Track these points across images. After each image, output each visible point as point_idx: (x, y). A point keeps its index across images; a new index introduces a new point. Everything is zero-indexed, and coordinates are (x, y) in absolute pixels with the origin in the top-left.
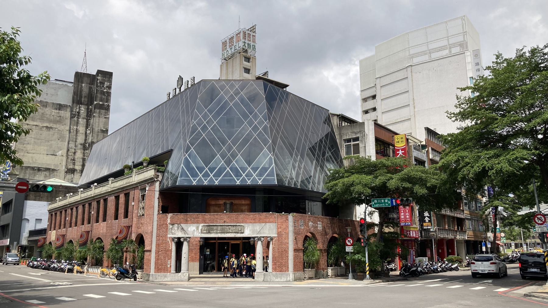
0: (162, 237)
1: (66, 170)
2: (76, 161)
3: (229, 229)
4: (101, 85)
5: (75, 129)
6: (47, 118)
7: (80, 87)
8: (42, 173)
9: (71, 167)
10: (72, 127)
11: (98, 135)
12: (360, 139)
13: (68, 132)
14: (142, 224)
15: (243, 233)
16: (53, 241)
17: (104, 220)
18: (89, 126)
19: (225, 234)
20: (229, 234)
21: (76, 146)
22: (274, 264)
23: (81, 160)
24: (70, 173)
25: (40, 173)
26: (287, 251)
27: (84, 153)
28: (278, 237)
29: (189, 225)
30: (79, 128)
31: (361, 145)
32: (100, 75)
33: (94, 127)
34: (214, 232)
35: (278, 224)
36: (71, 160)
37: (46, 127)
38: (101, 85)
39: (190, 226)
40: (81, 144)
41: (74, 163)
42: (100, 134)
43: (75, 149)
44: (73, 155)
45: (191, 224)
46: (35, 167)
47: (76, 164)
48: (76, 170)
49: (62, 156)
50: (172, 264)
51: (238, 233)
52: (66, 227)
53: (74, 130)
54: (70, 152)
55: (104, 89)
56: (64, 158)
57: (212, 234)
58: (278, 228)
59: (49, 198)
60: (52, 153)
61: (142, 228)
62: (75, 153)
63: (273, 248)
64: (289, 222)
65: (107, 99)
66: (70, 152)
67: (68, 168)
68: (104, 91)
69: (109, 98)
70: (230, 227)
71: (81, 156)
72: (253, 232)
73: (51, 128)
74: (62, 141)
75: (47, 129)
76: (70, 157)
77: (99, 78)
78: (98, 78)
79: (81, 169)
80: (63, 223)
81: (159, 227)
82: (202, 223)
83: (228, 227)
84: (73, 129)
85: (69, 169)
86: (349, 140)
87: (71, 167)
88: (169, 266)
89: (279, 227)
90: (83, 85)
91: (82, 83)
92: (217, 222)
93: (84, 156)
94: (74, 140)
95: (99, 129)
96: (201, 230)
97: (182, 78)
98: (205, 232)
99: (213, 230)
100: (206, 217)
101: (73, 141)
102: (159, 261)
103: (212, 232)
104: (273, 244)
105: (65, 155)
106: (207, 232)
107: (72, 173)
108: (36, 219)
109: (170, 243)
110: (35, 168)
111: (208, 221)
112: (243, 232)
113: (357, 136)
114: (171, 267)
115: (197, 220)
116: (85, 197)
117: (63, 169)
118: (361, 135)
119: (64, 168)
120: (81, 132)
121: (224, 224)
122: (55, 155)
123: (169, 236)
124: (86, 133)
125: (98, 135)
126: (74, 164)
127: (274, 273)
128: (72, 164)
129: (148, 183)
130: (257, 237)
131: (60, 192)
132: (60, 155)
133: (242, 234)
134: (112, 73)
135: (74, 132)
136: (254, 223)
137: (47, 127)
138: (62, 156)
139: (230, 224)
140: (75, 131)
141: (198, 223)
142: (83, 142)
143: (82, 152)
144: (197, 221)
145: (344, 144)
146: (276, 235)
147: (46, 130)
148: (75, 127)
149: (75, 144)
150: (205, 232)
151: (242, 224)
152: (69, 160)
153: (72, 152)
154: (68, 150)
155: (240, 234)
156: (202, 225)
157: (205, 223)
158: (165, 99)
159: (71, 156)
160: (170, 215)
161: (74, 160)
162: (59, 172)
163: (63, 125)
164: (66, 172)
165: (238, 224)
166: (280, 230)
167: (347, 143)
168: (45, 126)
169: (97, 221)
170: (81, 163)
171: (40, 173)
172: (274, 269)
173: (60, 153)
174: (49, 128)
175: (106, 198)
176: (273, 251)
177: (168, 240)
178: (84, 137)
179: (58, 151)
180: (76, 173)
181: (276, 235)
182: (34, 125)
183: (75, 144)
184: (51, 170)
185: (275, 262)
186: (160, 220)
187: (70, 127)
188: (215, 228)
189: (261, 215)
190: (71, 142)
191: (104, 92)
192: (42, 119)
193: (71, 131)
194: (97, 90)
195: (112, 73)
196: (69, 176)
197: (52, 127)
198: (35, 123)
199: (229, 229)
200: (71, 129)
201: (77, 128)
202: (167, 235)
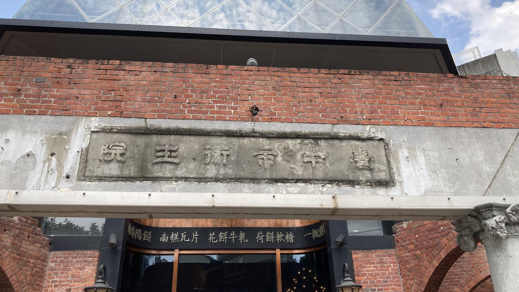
3: (289, 155)
19: (264, 186)
20: (293, 188)
34: (179, 173)
45: (15, 119)
51: (352, 183)
57: (166, 185)
70: (290, 143)
82: (98, 112)
83: (277, 145)
98: (114, 169)
103: (167, 171)
106: (131, 170)
112: (383, 176)
115: (64, 92)
121: (247, 126)
130: (502, 208)
133: (381, 191)
136: (447, 124)
139: (288, 128)
141: (66, 112)
150: (114, 169)
155: (367, 190)
156: (95, 123)
157: (121, 115)
165: (343, 130)
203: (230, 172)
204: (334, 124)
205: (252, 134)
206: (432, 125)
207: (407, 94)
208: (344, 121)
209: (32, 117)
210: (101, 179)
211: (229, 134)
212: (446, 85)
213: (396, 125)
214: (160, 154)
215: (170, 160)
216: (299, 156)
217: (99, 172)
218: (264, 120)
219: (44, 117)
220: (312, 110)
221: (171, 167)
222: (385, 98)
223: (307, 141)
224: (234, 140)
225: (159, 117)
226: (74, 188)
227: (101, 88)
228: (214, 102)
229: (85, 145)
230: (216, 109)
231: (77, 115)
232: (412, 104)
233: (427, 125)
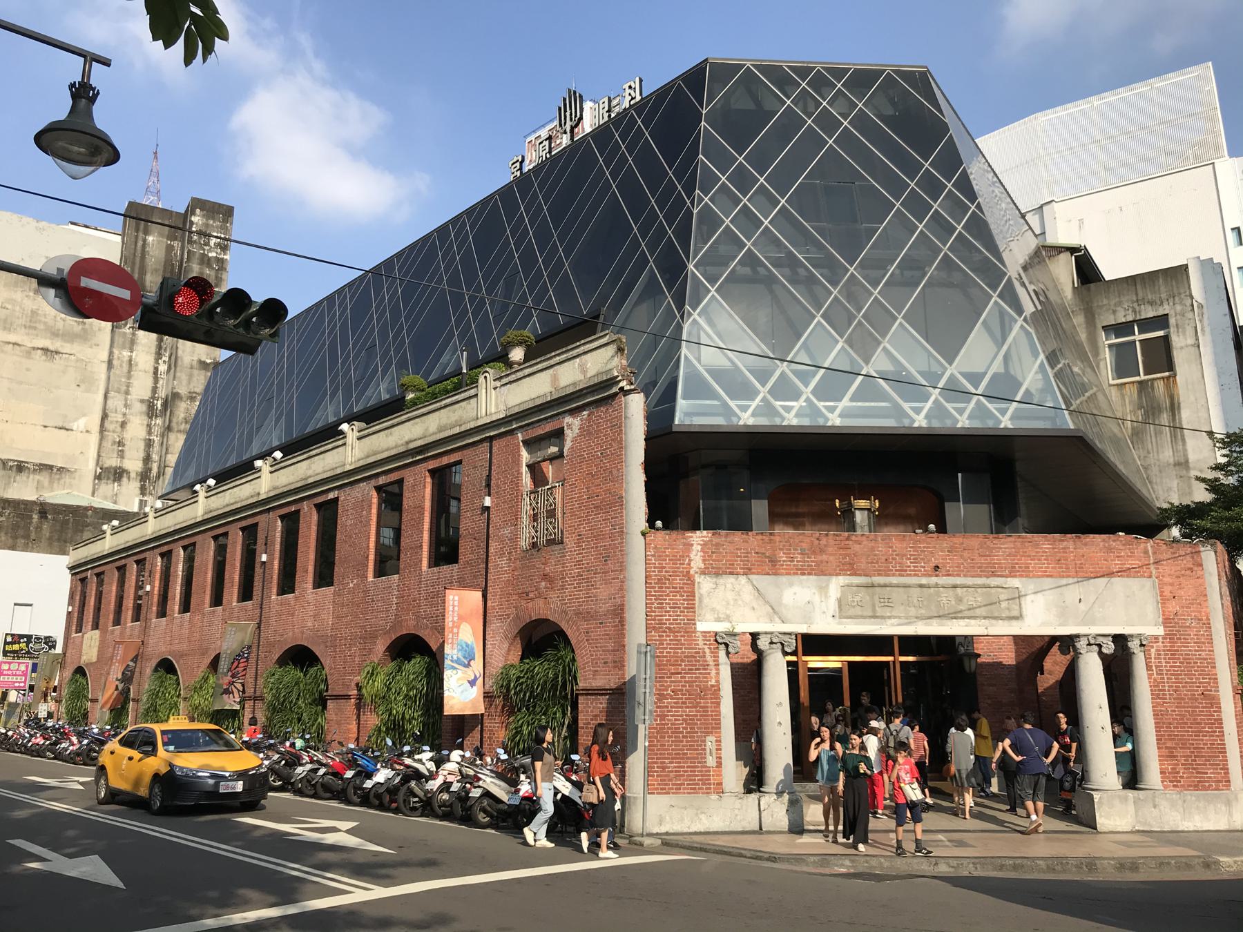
0: (669, 628)
1: (99, 470)
2: (126, 448)
4: (200, 238)
5: (126, 359)
6: (45, 323)
7: (140, 243)
8: (28, 477)
9: (112, 461)
10: (116, 351)
11: (190, 376)
12: (1172, 321)
13: (105, 366)
14: (545, 577)
15: (1019, 617)
16: (89, 664)
17: (324, 577)
18: (165, 350)
20: (962, 622)
21: (126, 406)
22: (1167, 755)
23: (142, 445)
24: (108, 479)
25: (25, 478)
26: (1213, 702)
27: (149, 426)
28: (1170, 636)
29: (784, 579)
30: (136, 356)
31: (1177, 341)
32: (198, 211)
33: (180, 352)
35: (1162, 584)
36: (114, 443)
37: (42, 349)
38: (200, 238)
39: (791, 585)
40: (142, 401)
41: (122, 451)
42: (196, 372)
43: (124, 415)
44: (119, 429)
46: (11, 460)
47: (127, 454)
48: (128, 472)
49: (87, 431)
50: (724, 754)
52: (142, 617)
53: (122, 362)
54: (111, 422)
55: (210, 251)
56: (94, 438)
57: (889, 622)
58: (1164, 600)
59: (56, 544)
60: (60, 425)
61: (551, 594)
62: (123, 425)
63: (1156, 686)
64: (1207, 575)
65: (217, 277)
66: (111, 422)
67: (106, 466)
68: (210, 255)
69: (223, 277)
70: (959, 590)
71: (142, 433)
72: (1063, 614)
73: (57, 353)
74: (88, 390)
75: (46, 355)
76: (112, 436)
77: (194, 219)
78: (193, 219)
79: (140, 470)
80: (129, 603)
81: (656, 583)
84: (119, 358)
85: (107, 468)
86: (1121, 329)
87: (114, 465)
88: (711, 761)
89: (1167, 593)
90: (150, 239)
91: (146, 233)
92: (902, 572)
93: (150, 433)
94: (124, 388)
95: (196, 358)
96: (840, 601)
97: (581, 96)
98: (858, 611)
99: (887, 602)
100: (857, 547)
101: (119, 393)
102: (667, 741)
104: (1149, 668)
105: (96, 428)
107: (114, 481)
108: (15, 604)
109: (708, 657)
110: (11, 464)
111: (863, 566)
112: (1016, 613)
113: (1161, 312)
114: (719, 764)
115: (820, 558)
116: (227, 505)
117: (89, 467)
118: (1178, 308)
119: (91, 464)
120: (141, 366)
122: (67, 430)
123: (701, 627)
124: (156, 369)
125: (190, 376)
126: (121, 455)
127: (1173, 794)
128: (115, 455)
129: (572, 412)
131: (87, 526)
132: (82, 427)
133: (1014, 623)
134: (233, 208)
135: (121, 366)
137: (45, 350)
138: (87, 431)
140: (124, 365)
141: (823, 573)
142: (147, 395)
143: (145, 423)
144: (818, 564)
145: (1106, 341)
146: (1160, 631)
147: (44, 357)
148: (126, 353)
149: (126, 400)
150: (858, 611)
151: (1015, 582)
152: (107, 444)
153: (117, 422)
154: (104, 417)
156: (842, 580)
157: (855, 574)
158: (505, 177)
159: (114, 432)
160: (698, 538)
161: (120, 443)
162: (77, 475)
163: (91, 347)
164: (98, 477)
166: (1173, 607)
167: (1116, 338)
168: (41, 346)
169: (287, 584)
170: (142, 454)
171: (25, 478)
172: (1171, 778)
173: (80, 424)
174: (52, 352)
175: (331, 496)
176: (1155, 697)
177: (701, 643)
178: (149, 382)
179: (76, 419)
180: (125, 480)
181: (1160, 631)
182: (9, 343)
183: (126, 400)
184: (55, 470)
185: (1169, 744)
186: (660, 558)
187: (111, 353)
188: (897, 595)
189: (1086, 544)
190: (112, 394)
191: (209, 259)
192: (30, 327)
193: (115, 362)
194: (189, 252)
195: (233, 208)
196: (108, 488)
197: (61, 350)
198: (12, 338)
199: (960, 600)
200: (115, 357)
201: (131, 356)
202: (692, 621)
203: (923, 611)
204: (987, 577)
205: (937, 586)
206: (1051, 576)
207: (1037, 552)
208: (994, 574)
209: (804, 577)
210: (850, 617)
211: (921, 586)
212: (1065, 543)
213: (1027, 576)
214: (882, 600)
215: (889, 604)
216: (965, 600)
217: (852, 612)
218: (943, 575)
219: (811, 577)
220: (973, 567)
221: (889, 609)
222: (1022, 556)
223: (970, 590)
224: (925, 589)
225: (879, 575)
226: (840, 623)
227: (840, 555)
228: (911, 563)
229: (839, 596)
230: (912, 568)
231: (830, 575)
232: (1039, 560)
233: (1048, 576)
